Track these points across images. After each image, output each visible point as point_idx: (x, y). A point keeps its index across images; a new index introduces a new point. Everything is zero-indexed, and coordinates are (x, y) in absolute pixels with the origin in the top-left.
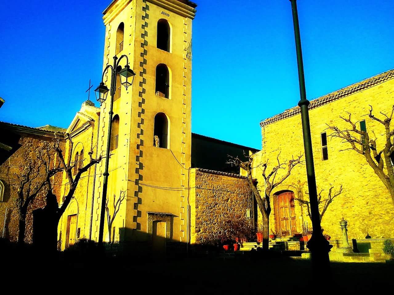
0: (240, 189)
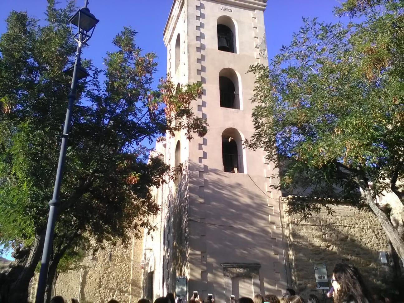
0: (363, 221)
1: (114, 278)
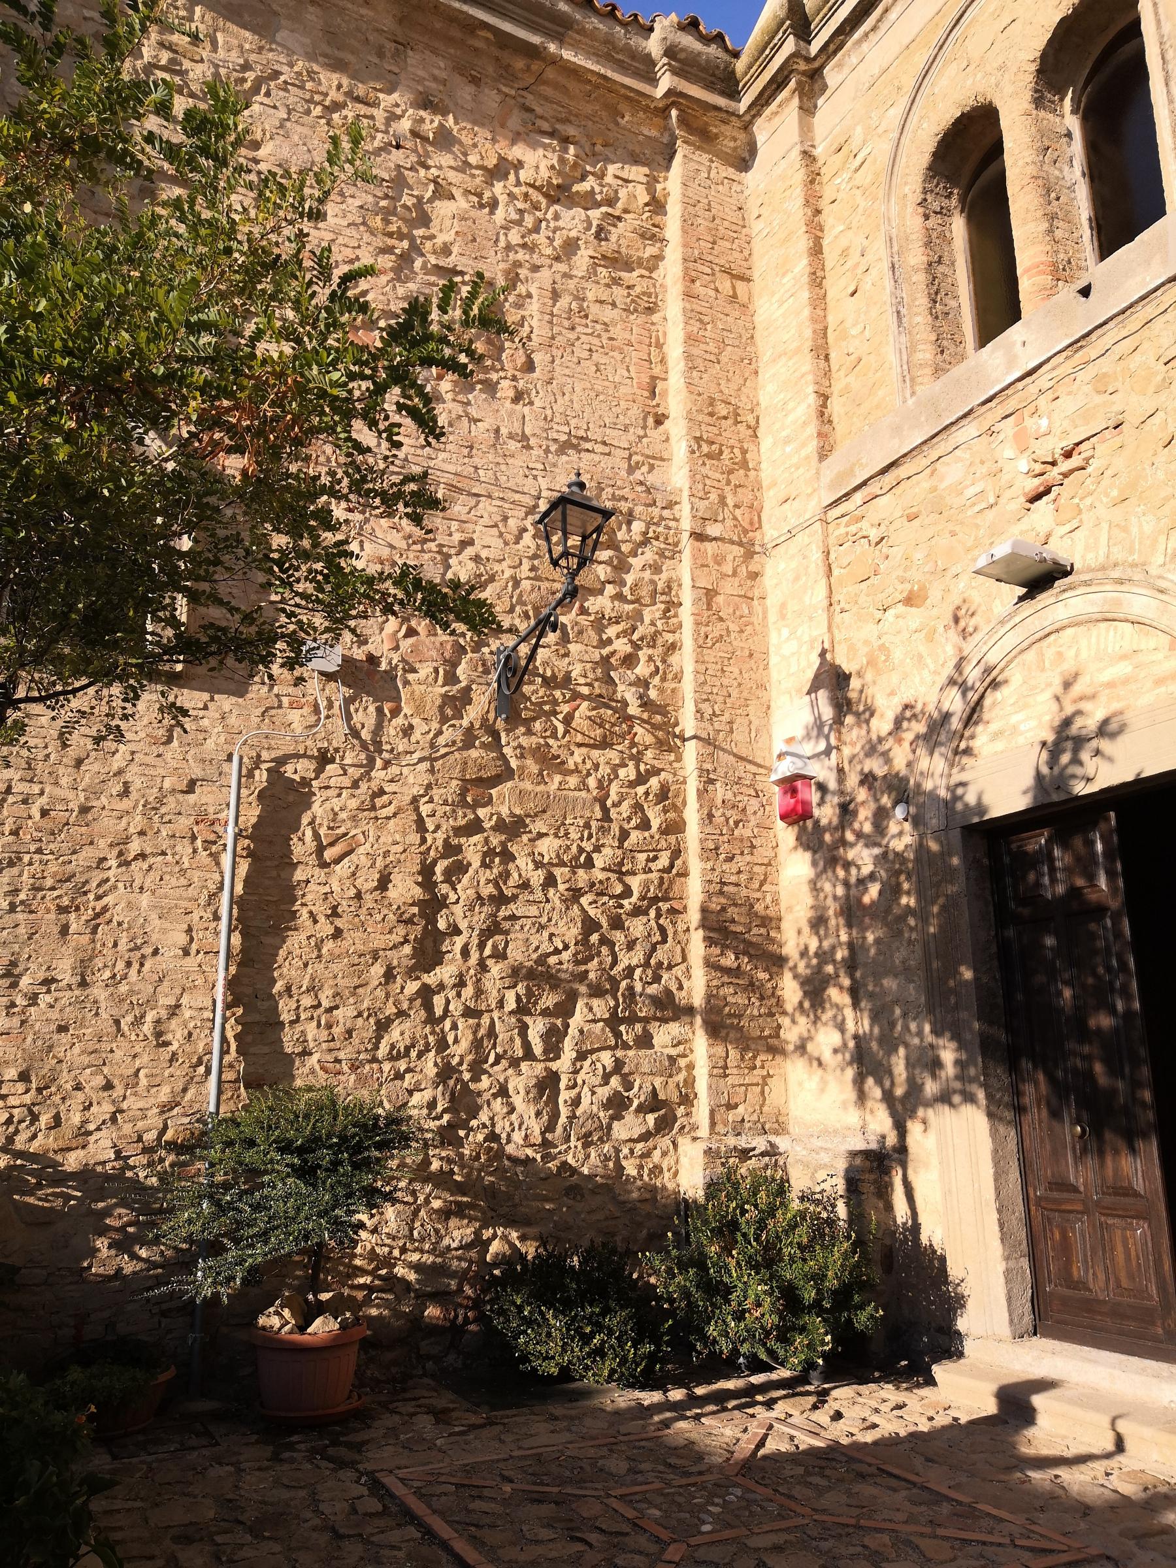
1: (550, 881)
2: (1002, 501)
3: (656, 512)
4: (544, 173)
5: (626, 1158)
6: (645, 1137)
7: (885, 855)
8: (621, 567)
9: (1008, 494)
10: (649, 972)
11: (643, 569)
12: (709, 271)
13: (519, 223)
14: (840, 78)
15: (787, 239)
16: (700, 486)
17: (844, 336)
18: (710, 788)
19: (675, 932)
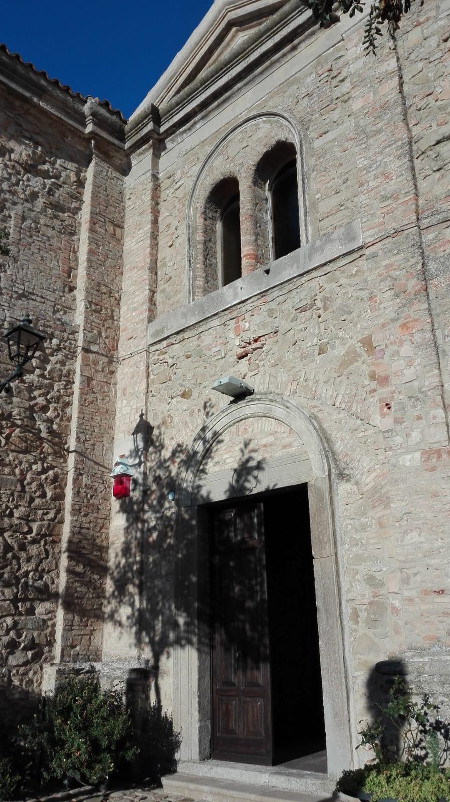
2: (227, 356)
3: (66, 335)
4: (24, 157)
5: (14, 675)
6: (25, 664)
7: (161, 518)
8: (45, 360)
9: (230, 354)
10: (37, 574)
11: (56, 363)
12: (103, 221)
13: (9, 179)
14: (172, 146)
15: (141, 214)
16: (89, 326)
17: (164, 265)
18: (80, 478)
19: (54, 553)
